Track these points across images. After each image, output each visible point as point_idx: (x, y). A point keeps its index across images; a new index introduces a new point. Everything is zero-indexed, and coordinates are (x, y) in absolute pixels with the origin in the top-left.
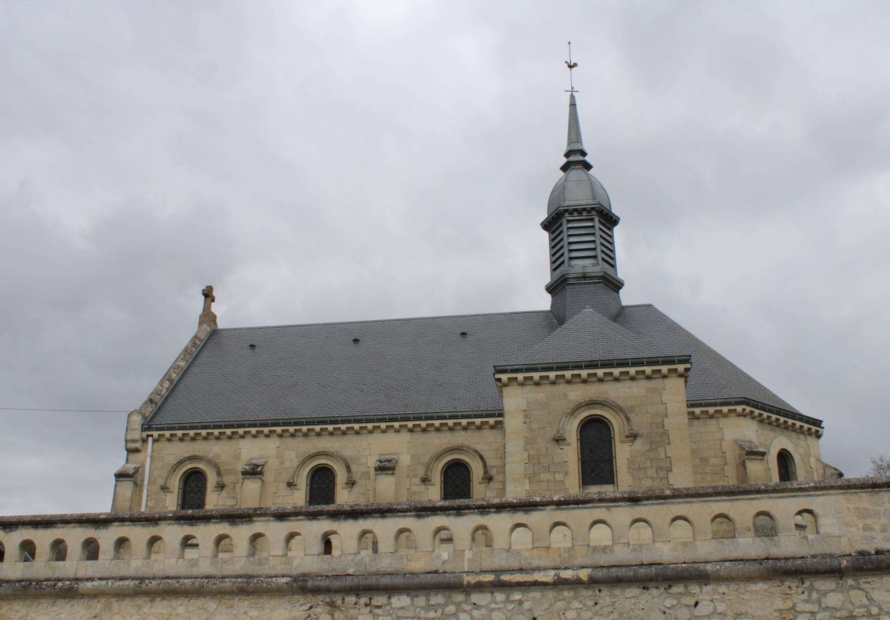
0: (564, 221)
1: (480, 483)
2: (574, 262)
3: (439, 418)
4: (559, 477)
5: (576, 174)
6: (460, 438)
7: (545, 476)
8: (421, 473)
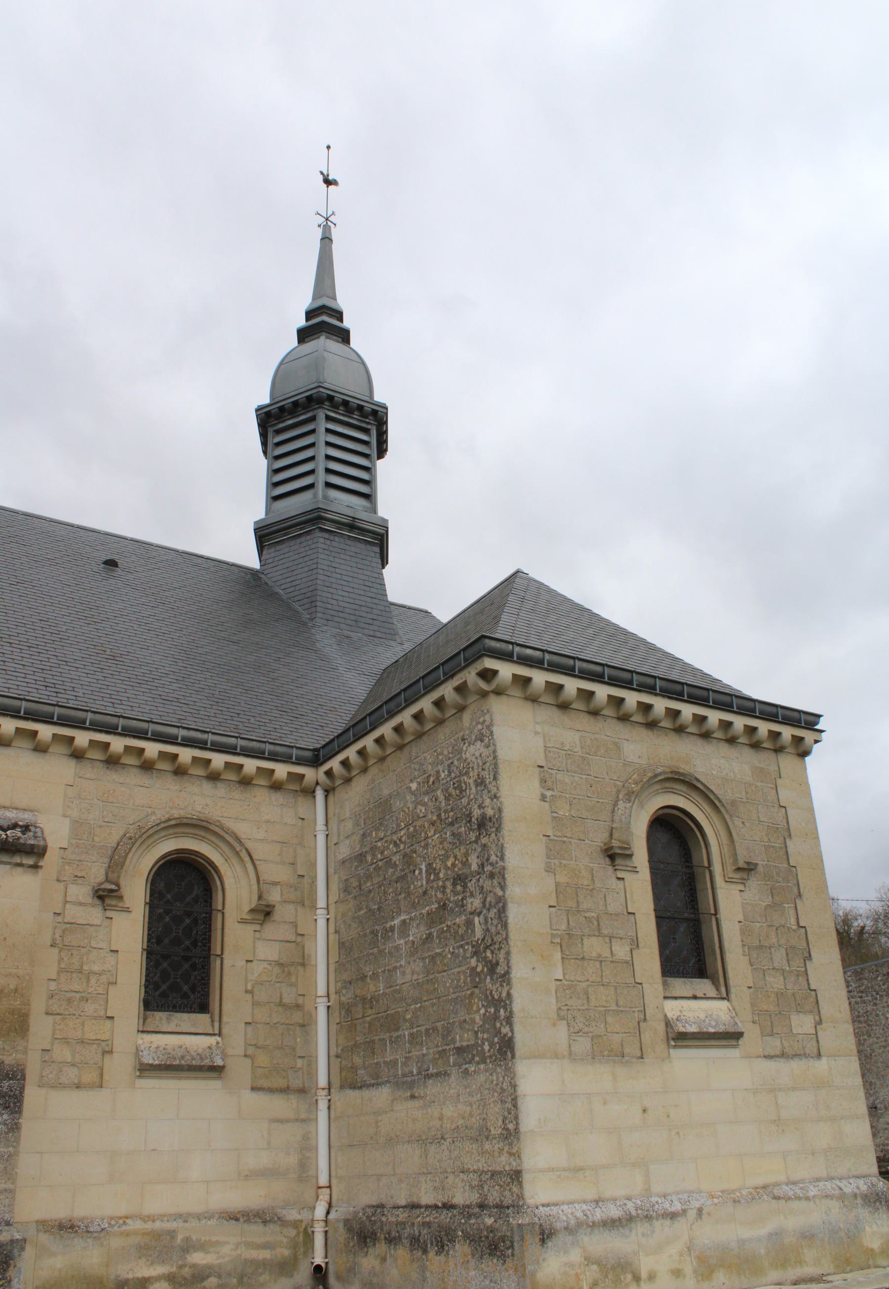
0: (321, 415)
1: (243, 921)
2: (333, 494)
3: (159, 738)
4: (621, 951)
5: (324, 343)
6: (199, 799)
7: (593, 946)
8: (97, 873)
